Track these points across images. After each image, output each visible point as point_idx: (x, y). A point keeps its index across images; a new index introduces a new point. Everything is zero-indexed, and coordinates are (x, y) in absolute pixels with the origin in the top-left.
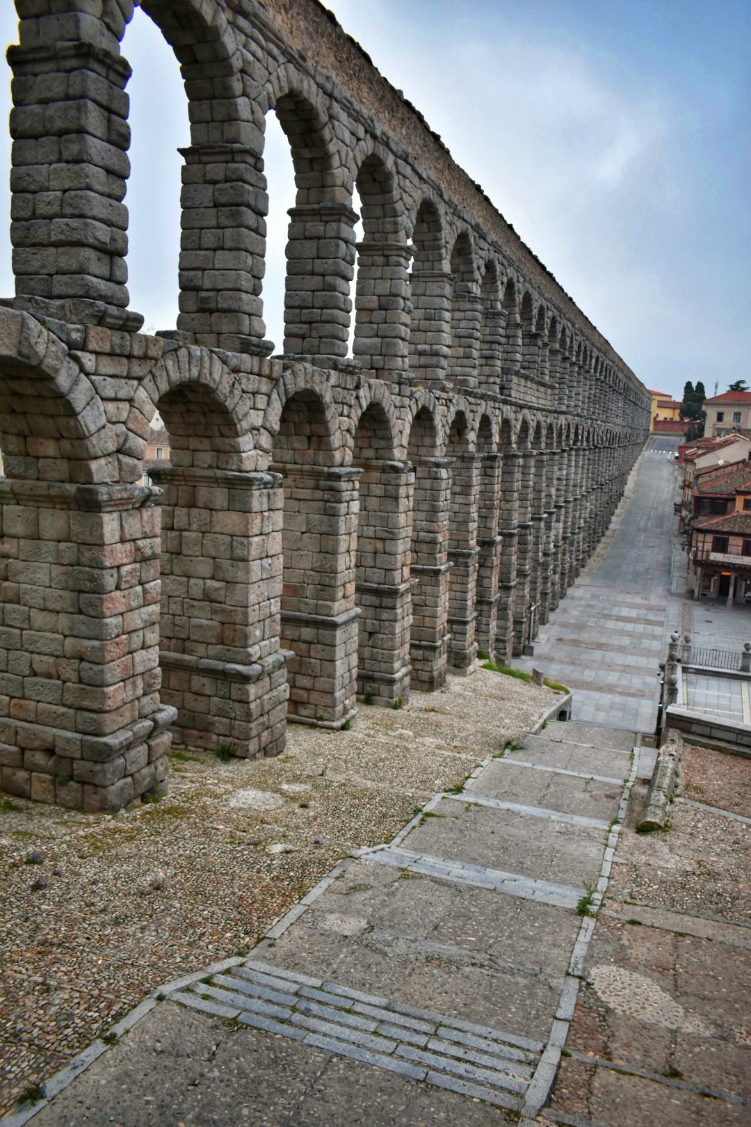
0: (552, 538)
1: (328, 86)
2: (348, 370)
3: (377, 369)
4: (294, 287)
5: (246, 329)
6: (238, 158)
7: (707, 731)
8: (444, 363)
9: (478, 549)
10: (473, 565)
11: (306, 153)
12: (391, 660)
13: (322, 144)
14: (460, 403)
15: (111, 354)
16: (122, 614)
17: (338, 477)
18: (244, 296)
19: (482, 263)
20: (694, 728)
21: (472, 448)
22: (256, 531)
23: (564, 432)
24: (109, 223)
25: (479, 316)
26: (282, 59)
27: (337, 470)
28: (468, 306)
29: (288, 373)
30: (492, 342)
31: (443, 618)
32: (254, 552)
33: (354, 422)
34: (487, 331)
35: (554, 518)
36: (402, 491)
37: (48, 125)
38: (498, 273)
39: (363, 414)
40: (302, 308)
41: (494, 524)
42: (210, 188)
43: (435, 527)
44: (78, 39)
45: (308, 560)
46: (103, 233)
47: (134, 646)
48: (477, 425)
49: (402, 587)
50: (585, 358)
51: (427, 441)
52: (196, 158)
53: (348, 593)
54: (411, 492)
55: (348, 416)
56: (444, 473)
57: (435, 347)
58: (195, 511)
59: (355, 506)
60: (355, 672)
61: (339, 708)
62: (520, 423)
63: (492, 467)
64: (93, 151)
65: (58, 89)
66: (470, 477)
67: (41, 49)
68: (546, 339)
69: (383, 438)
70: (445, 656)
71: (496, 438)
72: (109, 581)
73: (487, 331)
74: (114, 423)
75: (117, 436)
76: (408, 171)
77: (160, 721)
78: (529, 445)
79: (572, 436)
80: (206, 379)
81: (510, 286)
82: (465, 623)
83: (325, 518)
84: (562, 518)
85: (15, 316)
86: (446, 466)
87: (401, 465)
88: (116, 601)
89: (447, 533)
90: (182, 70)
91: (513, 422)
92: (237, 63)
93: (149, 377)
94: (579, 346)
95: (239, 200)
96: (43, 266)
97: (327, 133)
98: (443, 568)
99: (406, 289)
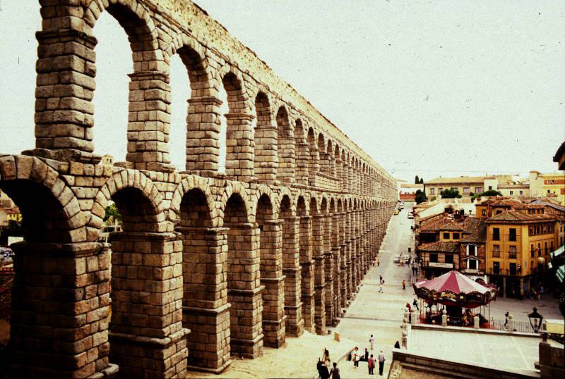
0: (345, 260)
1: (205, 43)
2: (221, 177)
4: (191, 137)
5: (160, 159)
6: (156, 77)
7: (413, 360)
8: (275, 171)
9: (300, 267)
10: (298, 277)
11: (195, 73)
12: (251, 332)
13: (202, 69)
15: (84, 175)
16: (86, 313)
17: (214, 233)
18: (159, 143)
20: (408, 359)
21: (294, 214)
22: (166, 264)
24: (84, 112)
25: (294, 147)
26: (179, 32)
28: (288, 142)
29: (184, 181)
30: (302, 159)
31: (281, 306)
32: (165, 275)
33: (223, 204)
34: (300, 153)
35: (346, 248)
36: (253, 239)
37: (54, 67)
38: (303, 125)
39: (229, 199)
41: (310, 253)
42: (143, 92)
43: (274, 256)
44: (70, 27)
45: (199, 278)
46: (80, 117)
47: (93, 331)
48: (296, 202)
49: (255, 291)
50: (357, 165)
51: (268, 211)
52: (135, 78)
53: (223, 295)
54: (258, 239)
56: (277, 228)
57: (270, 163)
58: (134, 255)
59: (225, 248)
60: (229, 340)
61: (220, 361)
62: (321, 199)
63: (307, 224)
65: (60, 50)
66: (294, 229)
67: (51, 33)
68: (334, 156)
69: (242, 212)
70: (284, 328)
71: (308, 208)
72: (79, 295)
73: (300, 153)
74: (83, 210)
75: (86, 217)
76: (249, 79)
77: (108, 373)
78: (328, 211)
79: (353, 204)
81: (311, 130)
82: (296, 309)
83: (209, 255)
85: (29, 160)
86: (278, 224)
87: (252, 225)
88: (83, 305)
89: (281, 260)
90: (129, 39)
91: (317, 200)
92: (155, 35)
93: (105, 186)
94: (353, 158)
95: (156, 97)
96: (49, 134)
97: (204, 64)
98: (279, 279)
99: (251, 135)
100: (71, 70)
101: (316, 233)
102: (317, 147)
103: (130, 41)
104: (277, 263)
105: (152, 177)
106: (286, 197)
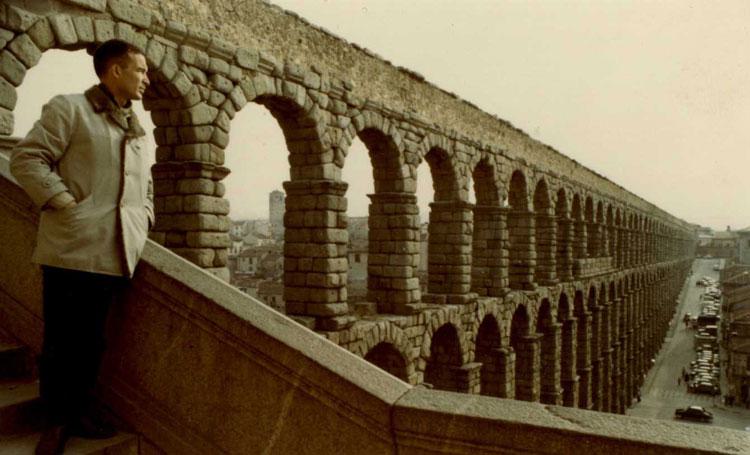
1: (453, 136)
3: (487, 287)
13: (450, 169)
14: (543, 292)
19: (555, 193)
21: (554, 320)
23: (623, 283)
27: (465, 367)
39: (481, 326)
40: (438, 264)
44: (323, 179)
48: (557, 303)
50: (636, 222)
54: (513, 366)
55: (472, 330)
64: (330, 237)
71: (572, 307)
79: (630, 283)
80: (389, 340)
84: (625, 347)
86: (535, 341)
87: (506, 351)
89: (539, 387)
91: (584, 291)
92: (401, 150)
97: (453, 162)
100: (325, 227)
101: (581, 339)
102: (583, 217)
103: (373, 165)
104: (535, 391)
105: (403, 323)
106: (545, 302)
